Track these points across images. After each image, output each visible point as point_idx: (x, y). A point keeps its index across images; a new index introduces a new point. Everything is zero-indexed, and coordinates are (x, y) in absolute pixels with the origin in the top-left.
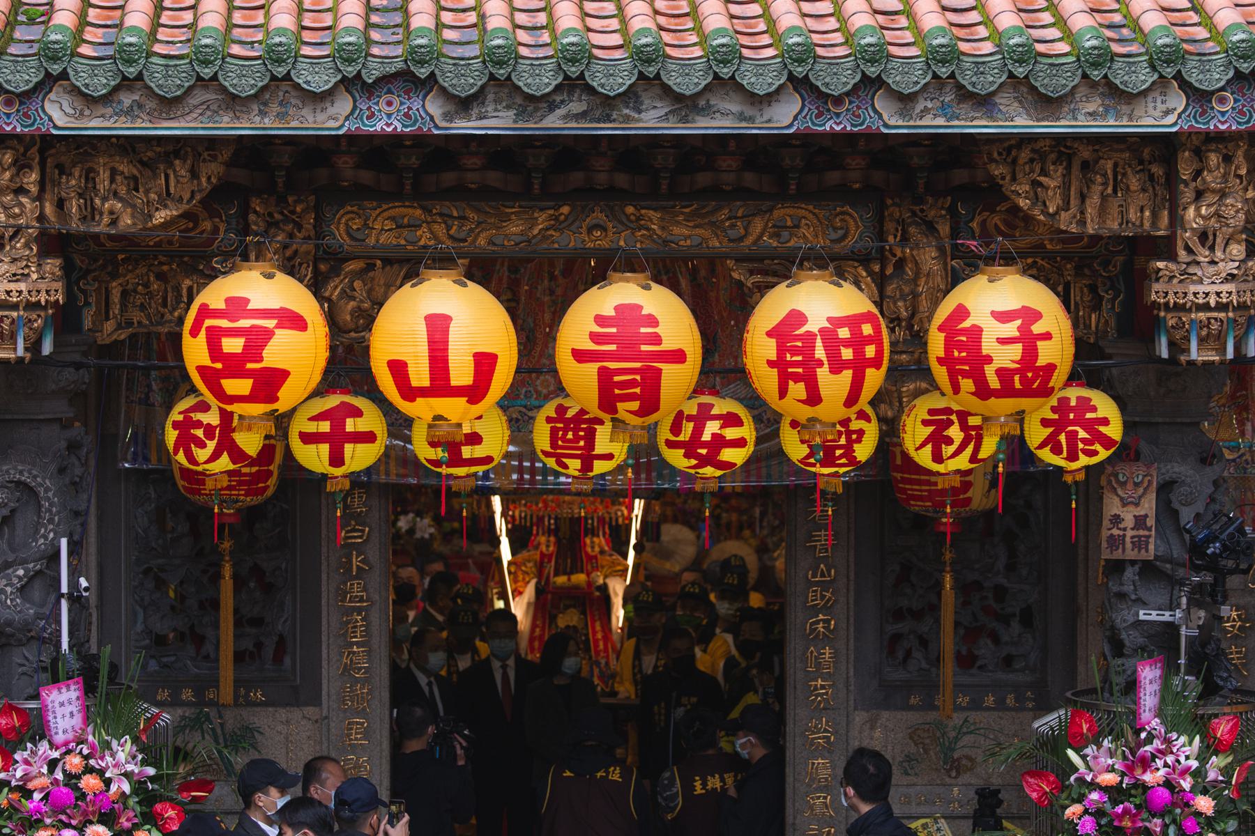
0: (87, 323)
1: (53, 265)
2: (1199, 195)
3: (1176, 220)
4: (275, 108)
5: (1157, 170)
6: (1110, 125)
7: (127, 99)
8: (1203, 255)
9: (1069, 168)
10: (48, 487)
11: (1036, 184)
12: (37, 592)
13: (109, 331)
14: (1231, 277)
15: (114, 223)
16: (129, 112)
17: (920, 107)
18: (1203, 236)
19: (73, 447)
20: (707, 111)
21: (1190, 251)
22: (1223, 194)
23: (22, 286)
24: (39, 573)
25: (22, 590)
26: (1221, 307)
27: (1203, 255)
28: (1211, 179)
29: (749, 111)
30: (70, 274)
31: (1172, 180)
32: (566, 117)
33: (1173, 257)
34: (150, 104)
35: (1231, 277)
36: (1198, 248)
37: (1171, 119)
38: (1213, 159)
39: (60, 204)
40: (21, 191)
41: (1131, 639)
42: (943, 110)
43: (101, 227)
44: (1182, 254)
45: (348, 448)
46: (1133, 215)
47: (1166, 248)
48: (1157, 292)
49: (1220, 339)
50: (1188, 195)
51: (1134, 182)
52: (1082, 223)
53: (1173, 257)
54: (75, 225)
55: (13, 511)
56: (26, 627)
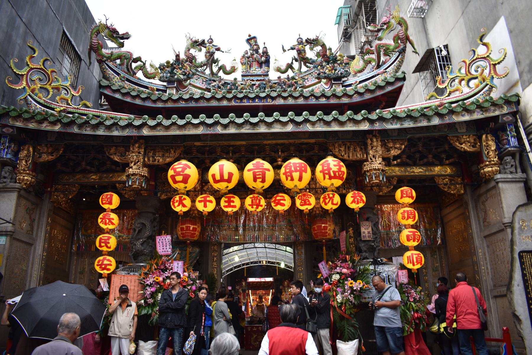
0: (159, 195)
1: (145, 169)
2: (372, 147)
3: (367, 154)
4: (188, 129)
5: (363, 147)
6: (354, 128)
7: (159, 128)
8: (374, 159)
9: (345, 147)
10: (148, 224)
11: (340, 150)
12: (145, 245)
13: (163, 197)
14: (380, 164)
15: (158, 162)
16: (159, 131)
17: (316, 125)
18: (374, 156)
19: (155, 219)
20: (274, 128)
21: (371, 159)
22: (377, 147)
23: (138, 171)
24: (145, 241)
25: (142, 244)
26: (379, 169)
27: (374, 159)
28: (375, 144)
29: (282, 128)
30: (150, 172)
31: (365, 145)
32: (245, 130)
33: (368, 161)
34: (163, 129)
35: (380, 164)
36: (373, 158)
37: (366, 127)
38: (375, 140)
39: (149, 160)
40: (139, 153)
41: (364, 248)
42: (320, 127)
43: (156, 163)
44: (369, 160)
45: (203, 203)
46: (358, 155)
47: (367, 160)
48: (365, 169)
49: (379, 176)
50: (370, 148)
51: (358, 149)
52: (349, 157)
53: (368, 161)
54: (151, 162)
55: (141, 229)
56: (142, 251)
